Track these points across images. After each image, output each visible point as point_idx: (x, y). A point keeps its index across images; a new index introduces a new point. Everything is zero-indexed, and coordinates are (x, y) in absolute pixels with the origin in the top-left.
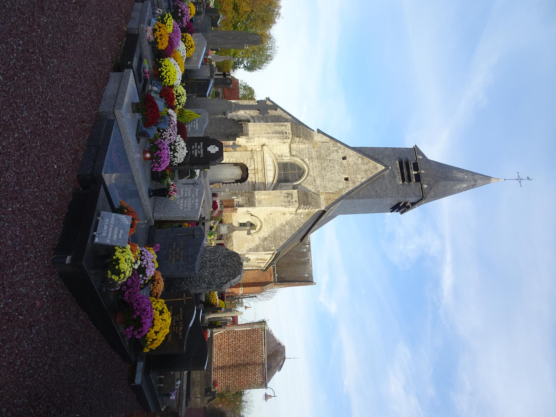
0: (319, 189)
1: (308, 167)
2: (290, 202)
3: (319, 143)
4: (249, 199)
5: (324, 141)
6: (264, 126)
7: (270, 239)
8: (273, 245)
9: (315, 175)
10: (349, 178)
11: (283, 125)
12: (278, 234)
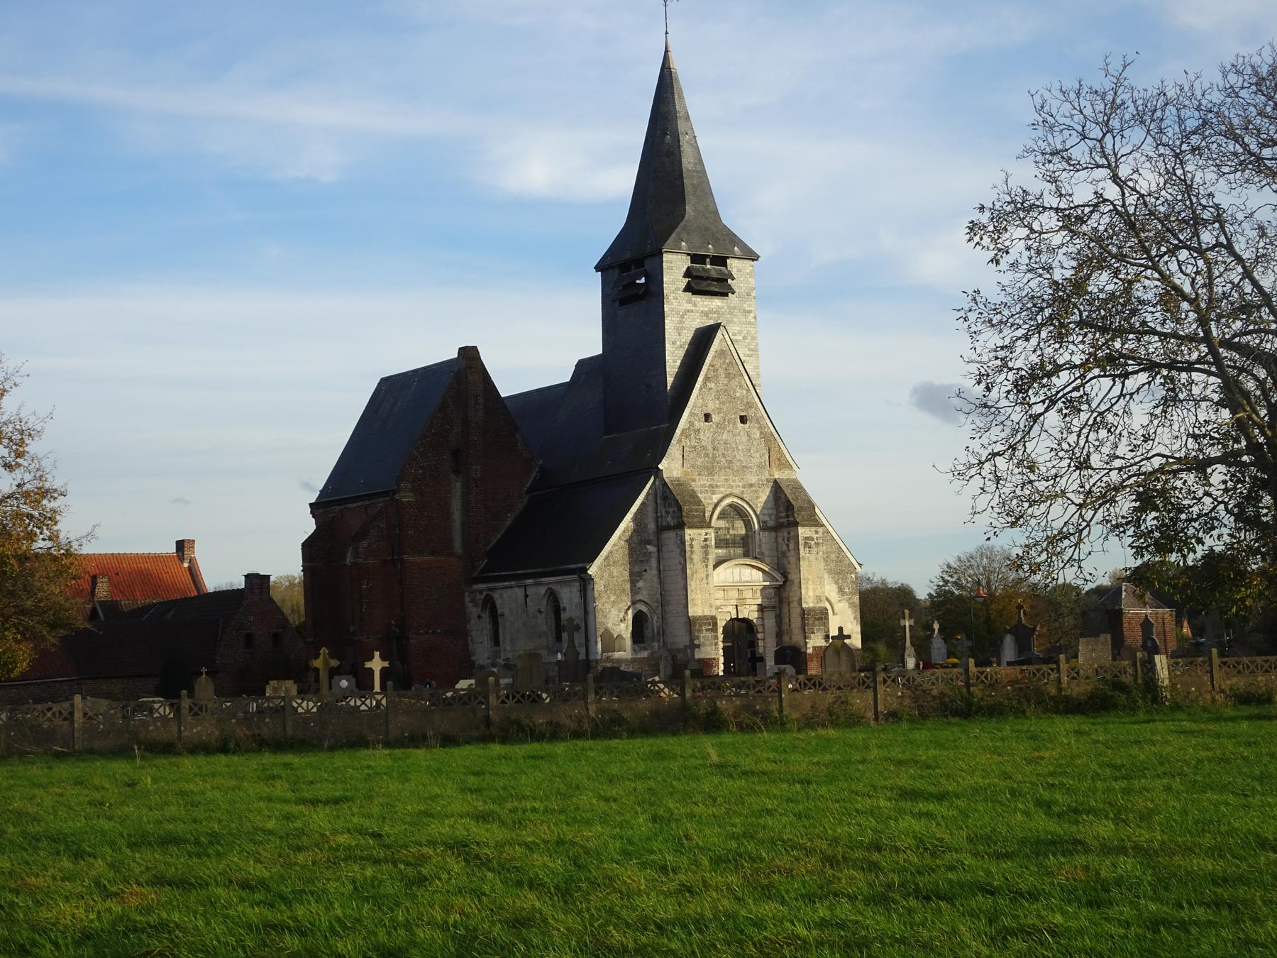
0: (764, 478)
1: (727, 496)
2: (818, 544)
4: (818, 619)
5: (681, 457)
6: (693, 583)
7: (840, 581)
8: (849, 576)
9: (741, 484)
10: (743, 414)
11: (692, 546)
12: (832, 565)
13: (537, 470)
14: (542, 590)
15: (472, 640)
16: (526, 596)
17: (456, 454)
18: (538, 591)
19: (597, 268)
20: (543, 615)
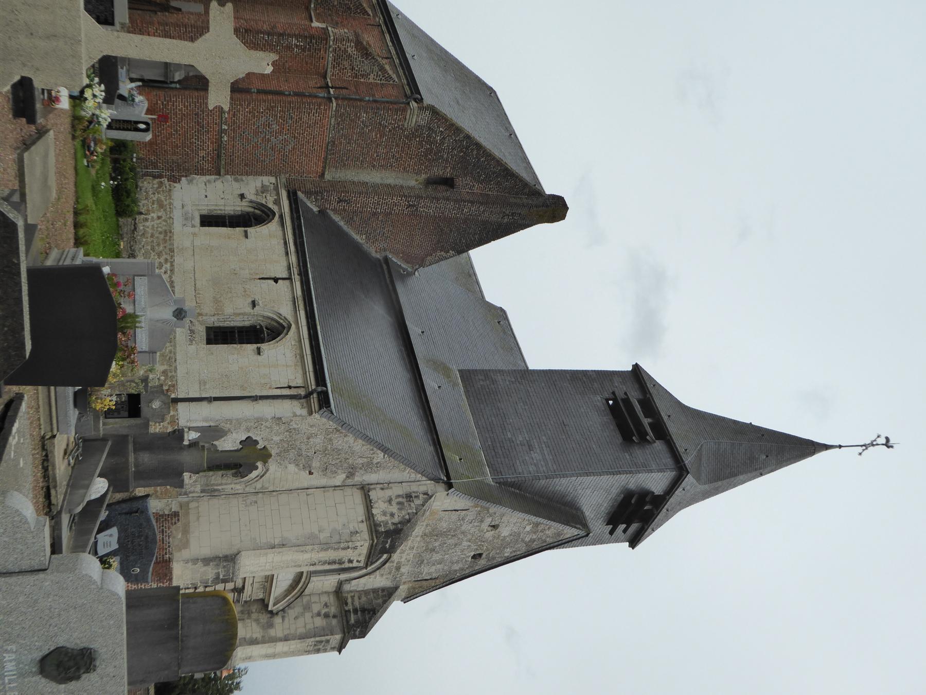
3: (441, 513)
13: (409, 269)
14: (286, 311)
15: (209, 181)
16: (276, 280)
17: (448, 182)
19: (636, 363)
20: (248, 309)
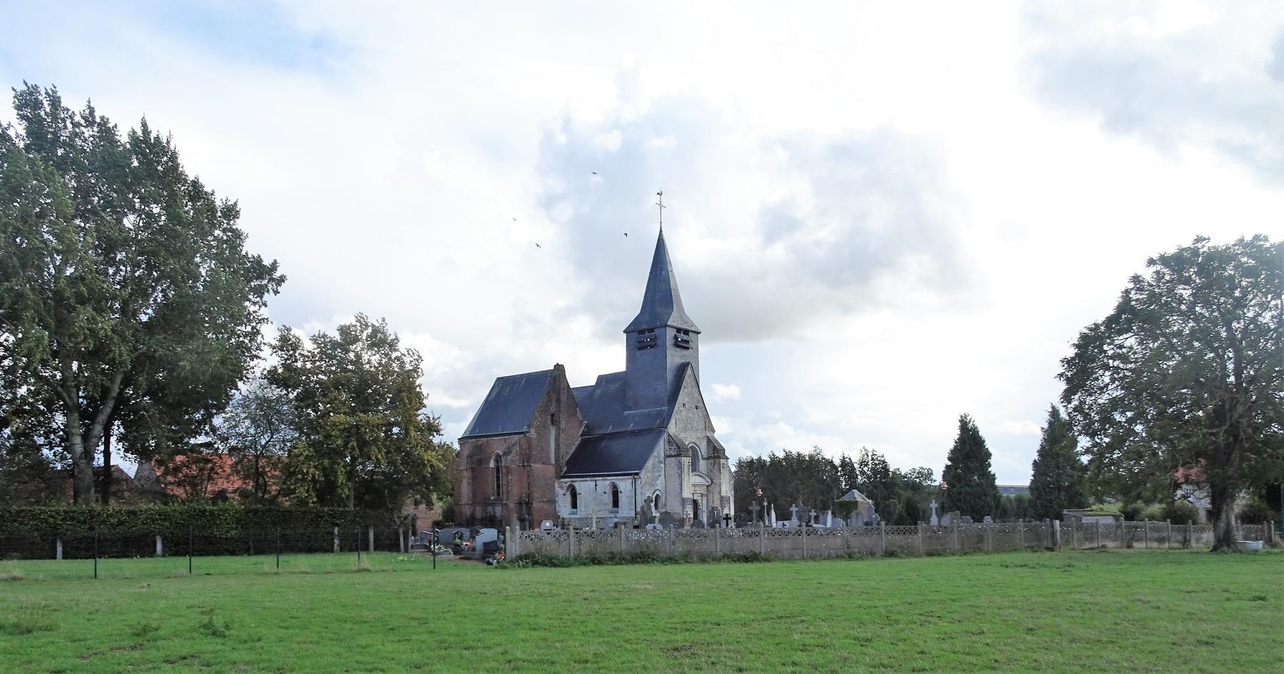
14: (607, 483)
16: (596, 485)
18: (604, 484)
19: (624, 332)
